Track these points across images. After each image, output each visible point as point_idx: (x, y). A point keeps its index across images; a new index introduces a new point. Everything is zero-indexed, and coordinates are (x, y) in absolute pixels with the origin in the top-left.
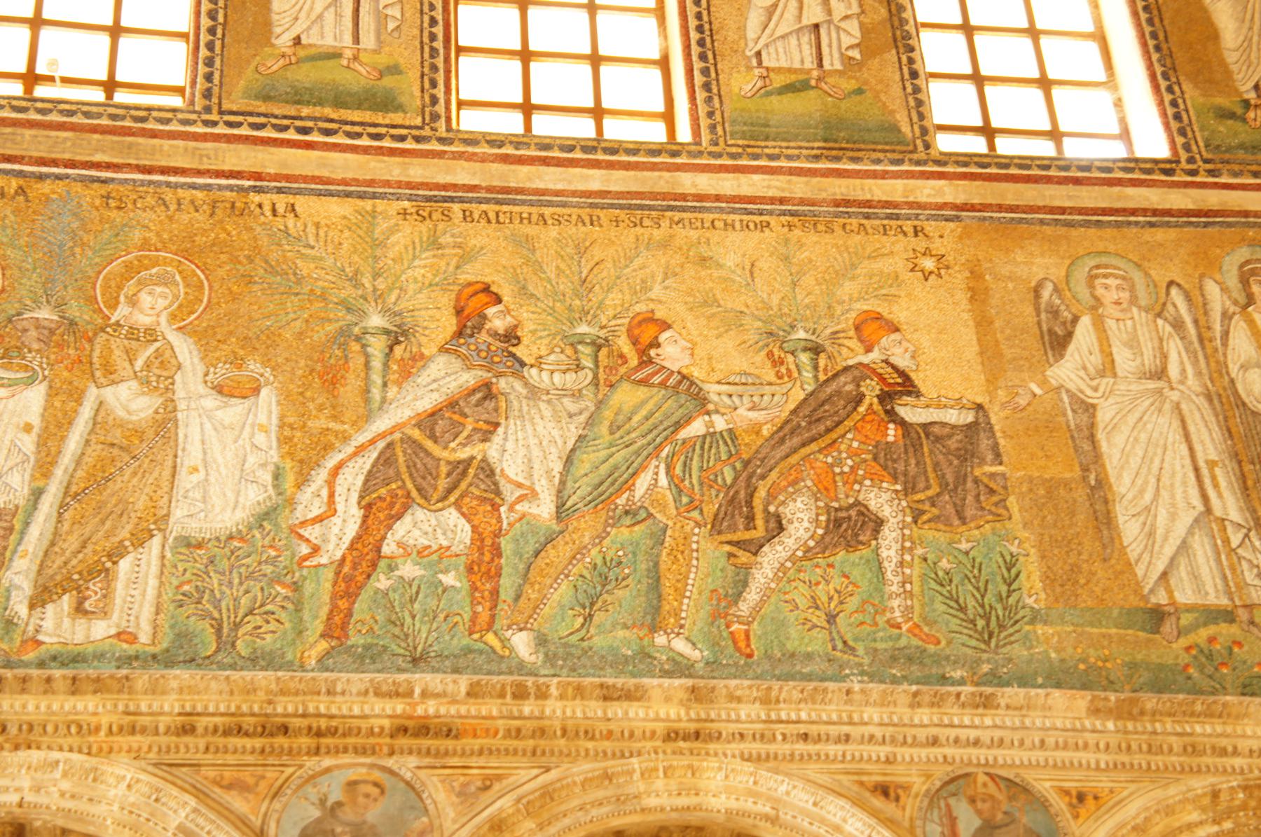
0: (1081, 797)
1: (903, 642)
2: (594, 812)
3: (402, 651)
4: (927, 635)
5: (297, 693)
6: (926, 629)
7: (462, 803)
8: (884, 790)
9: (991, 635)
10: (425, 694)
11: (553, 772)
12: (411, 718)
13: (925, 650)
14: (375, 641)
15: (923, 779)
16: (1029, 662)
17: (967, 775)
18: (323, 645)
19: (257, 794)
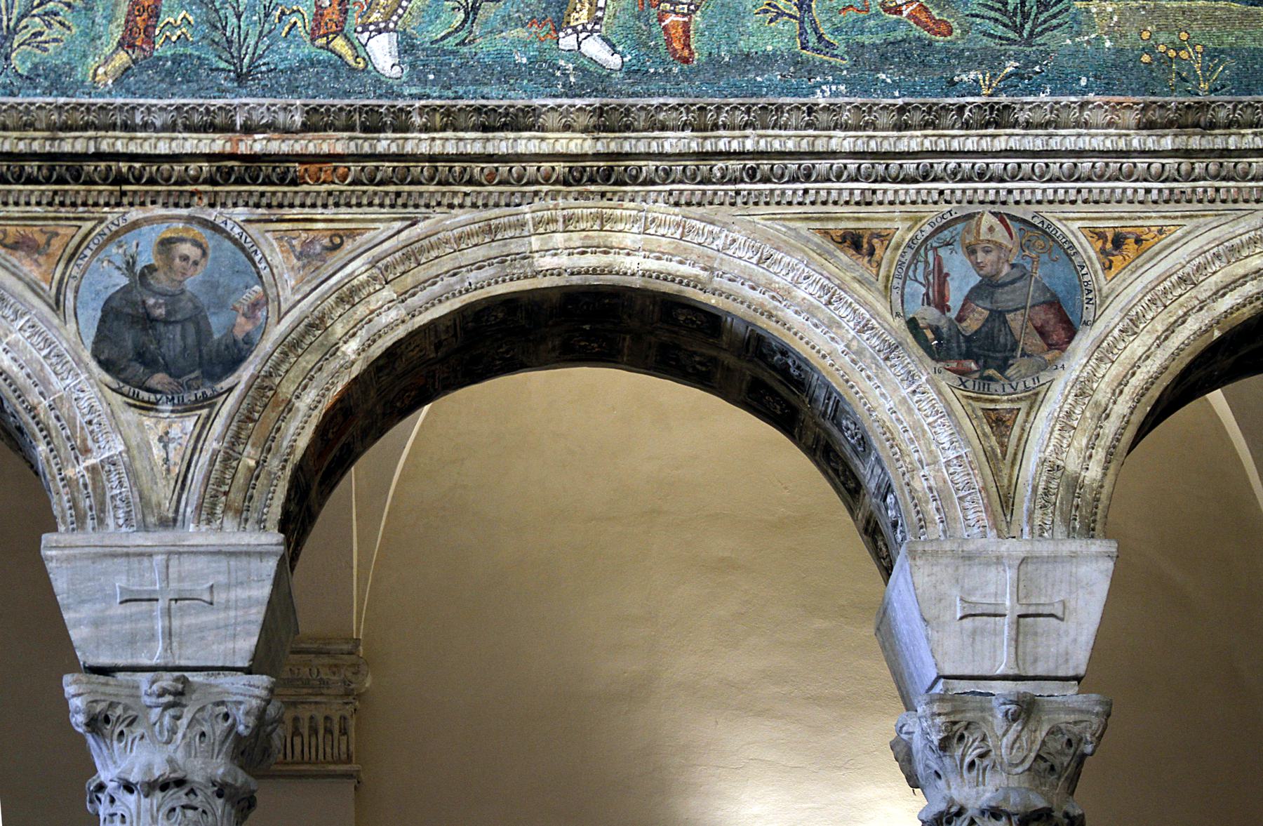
0: (1118, 241)
1: (899, 34)
2: (474, 277)
3: (223, 65)
4: (937, 22)
5: (85, 127)
6: (934, 13)
7: (304, 267)
8: (854, 242)
9: (1025, 16)
10: (248, 129)
11: (421, 225)
12: (233, 156)
13: (930, 44)
14: (189, 51)
15: (909, 224)
16: (1073, 55)
17: (970, 217)
18: (122, 58)
19: (48, 255)
